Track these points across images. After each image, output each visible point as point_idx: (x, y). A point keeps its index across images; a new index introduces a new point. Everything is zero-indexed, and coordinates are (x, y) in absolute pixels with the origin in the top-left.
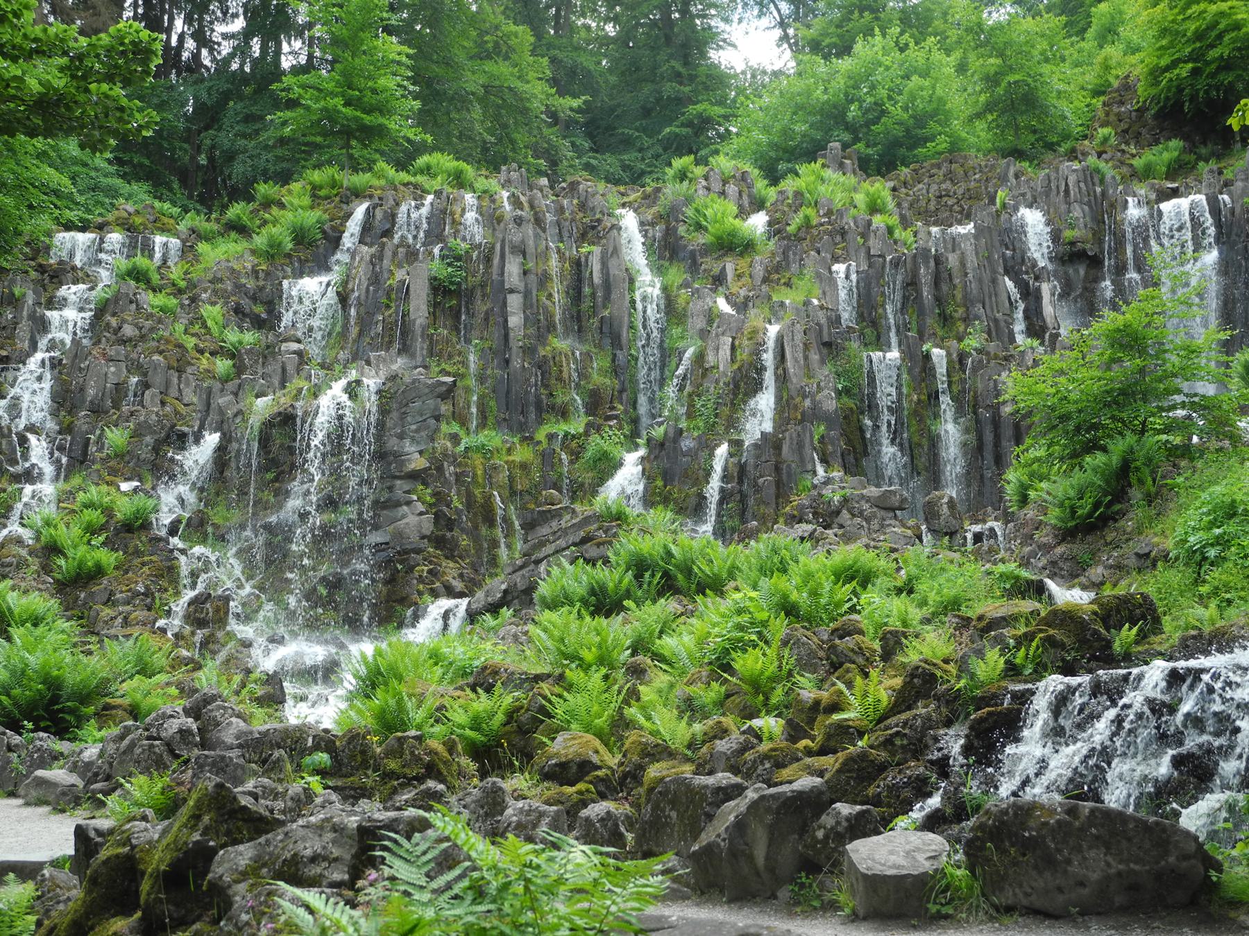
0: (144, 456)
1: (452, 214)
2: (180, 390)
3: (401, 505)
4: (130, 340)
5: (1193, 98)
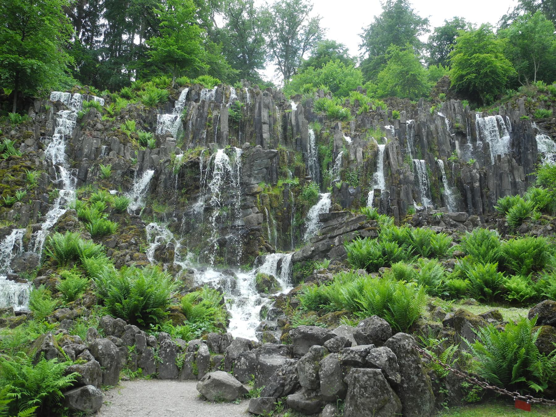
0: (118, 179)
1: (226, 94)
2: (124, 153)
3: (249, 208)
5: (474, 85)
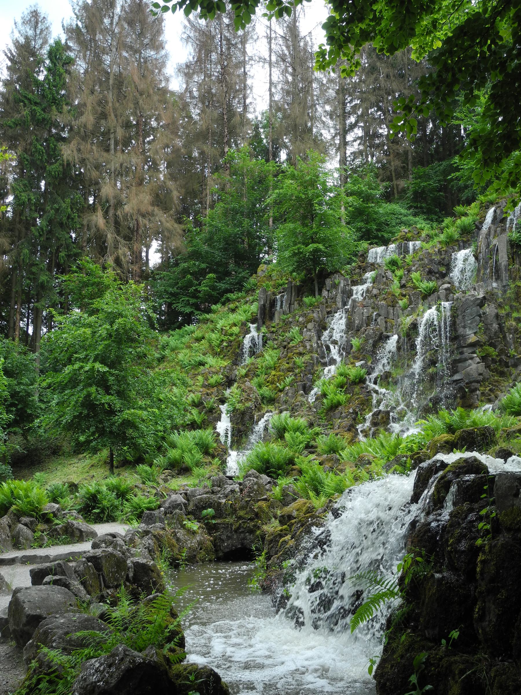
4: (375, 296)
